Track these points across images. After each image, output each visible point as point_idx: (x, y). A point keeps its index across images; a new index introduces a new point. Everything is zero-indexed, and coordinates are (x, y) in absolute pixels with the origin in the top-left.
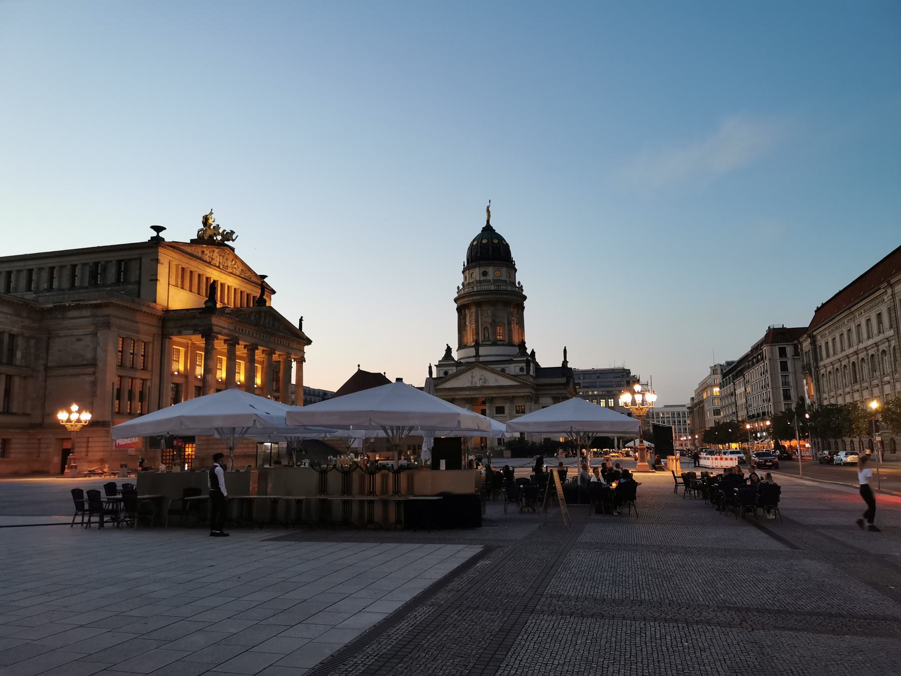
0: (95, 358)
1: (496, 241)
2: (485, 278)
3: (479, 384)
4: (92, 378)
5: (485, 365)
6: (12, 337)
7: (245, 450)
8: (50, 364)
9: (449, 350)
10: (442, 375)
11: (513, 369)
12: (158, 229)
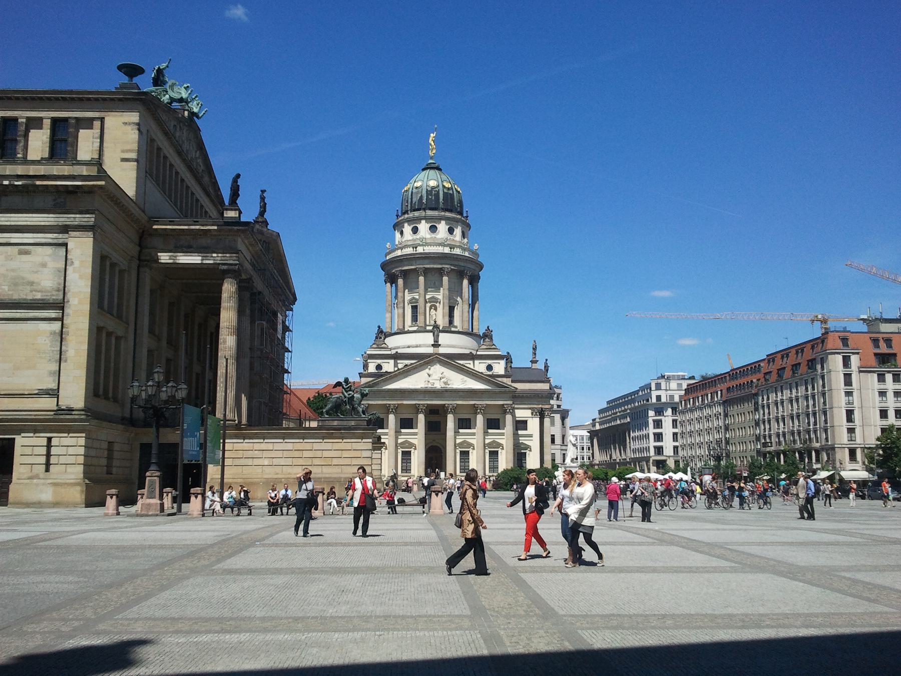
3: (438, 385)
4: (57, 326)
11: (480, 367)
12: (132, 71)
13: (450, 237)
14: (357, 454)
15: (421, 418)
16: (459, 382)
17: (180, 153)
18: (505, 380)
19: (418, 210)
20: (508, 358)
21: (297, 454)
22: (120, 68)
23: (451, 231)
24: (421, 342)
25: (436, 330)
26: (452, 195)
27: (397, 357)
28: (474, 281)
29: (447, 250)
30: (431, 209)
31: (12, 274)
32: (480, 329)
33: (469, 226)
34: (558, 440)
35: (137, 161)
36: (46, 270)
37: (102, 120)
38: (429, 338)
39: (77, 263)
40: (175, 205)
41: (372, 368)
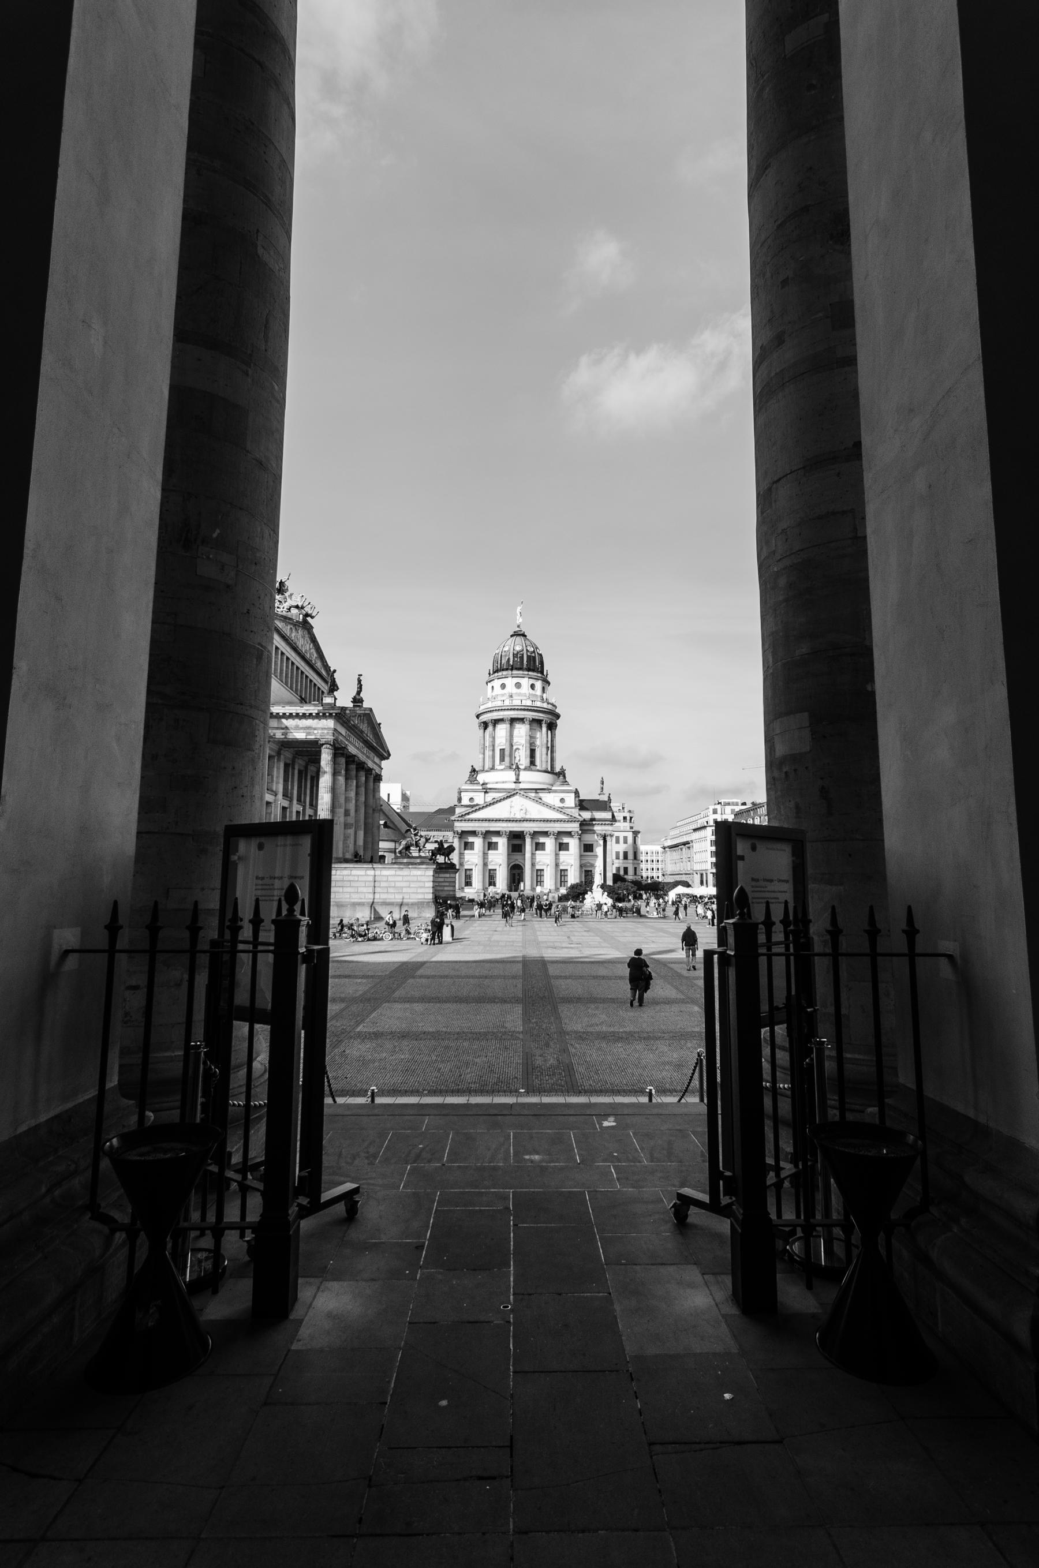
3: (518, 816)
9: (474, 770)
16: (536, 811)
20: (577, 793)
23: (533, 686)
26: (534, 658)
28: (552, 727)
29: (529, 703)
32: (557, 769)
33: (549, 683)
40: (291, 688)
41: (465, 801)
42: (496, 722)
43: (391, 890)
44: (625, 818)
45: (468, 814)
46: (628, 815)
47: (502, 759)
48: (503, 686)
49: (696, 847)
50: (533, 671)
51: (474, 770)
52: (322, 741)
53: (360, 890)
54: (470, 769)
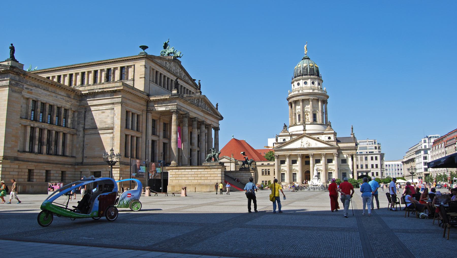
0: (113, 123)
1: (310, 64)
2: (306, 86)
3: (306, 146)
4: (112, 135)
5: (309, 136)
6: (66, 110)
7: (199, 181)
8: (86, 127)
10: (282, 141)
11: (324, 138)
12: (144, 48)
13: (312, 85)
14: (216, 175)
15: (299, 160)
16: (314, 144)
17: (169, 71)
18: (333, 143)
19: (300, 76)
21: (196, 176)
22: (140, 47)
23: (313, 83)
24: (298, 129)
25: (304, 124)
26: (313, 69)
27: (291, 136)
28: (324, 102)
29: (311, 91)
30: (305, 75)
31: (100, 120)
34: (379, 166)
35: (145, 78)
36: (109, 118)
37: (134, 65)
38: (302, 127)
39: (117, 115)
42: (296, 102)
43: (202, 178)
44: (376, 148)
45: (281, 147)
46: (377, 145)
47: (299, 120)
48: (298, 84)
49: (417, 161)
50: (313, 75)
51: (285, 126)
52: (172, 111)
53: (189, 178)
54: (283, 125)
